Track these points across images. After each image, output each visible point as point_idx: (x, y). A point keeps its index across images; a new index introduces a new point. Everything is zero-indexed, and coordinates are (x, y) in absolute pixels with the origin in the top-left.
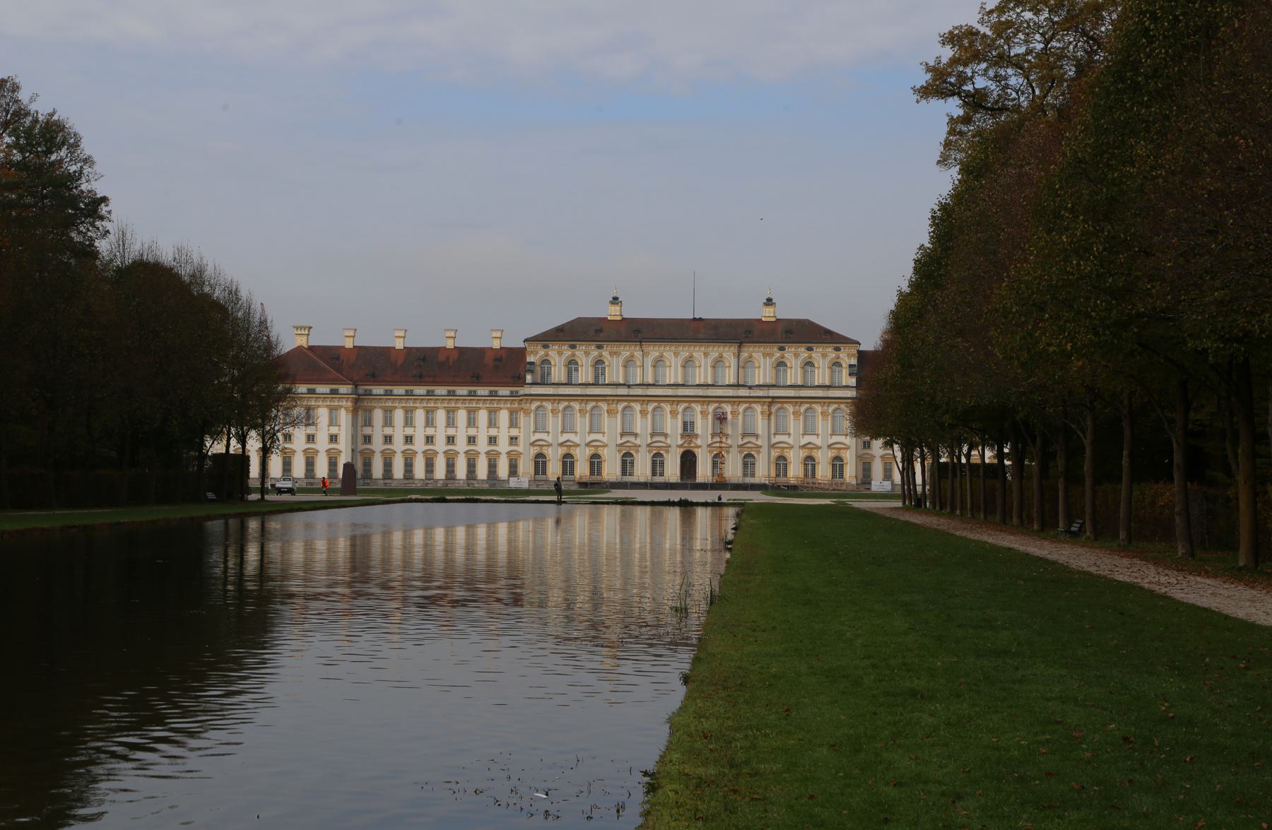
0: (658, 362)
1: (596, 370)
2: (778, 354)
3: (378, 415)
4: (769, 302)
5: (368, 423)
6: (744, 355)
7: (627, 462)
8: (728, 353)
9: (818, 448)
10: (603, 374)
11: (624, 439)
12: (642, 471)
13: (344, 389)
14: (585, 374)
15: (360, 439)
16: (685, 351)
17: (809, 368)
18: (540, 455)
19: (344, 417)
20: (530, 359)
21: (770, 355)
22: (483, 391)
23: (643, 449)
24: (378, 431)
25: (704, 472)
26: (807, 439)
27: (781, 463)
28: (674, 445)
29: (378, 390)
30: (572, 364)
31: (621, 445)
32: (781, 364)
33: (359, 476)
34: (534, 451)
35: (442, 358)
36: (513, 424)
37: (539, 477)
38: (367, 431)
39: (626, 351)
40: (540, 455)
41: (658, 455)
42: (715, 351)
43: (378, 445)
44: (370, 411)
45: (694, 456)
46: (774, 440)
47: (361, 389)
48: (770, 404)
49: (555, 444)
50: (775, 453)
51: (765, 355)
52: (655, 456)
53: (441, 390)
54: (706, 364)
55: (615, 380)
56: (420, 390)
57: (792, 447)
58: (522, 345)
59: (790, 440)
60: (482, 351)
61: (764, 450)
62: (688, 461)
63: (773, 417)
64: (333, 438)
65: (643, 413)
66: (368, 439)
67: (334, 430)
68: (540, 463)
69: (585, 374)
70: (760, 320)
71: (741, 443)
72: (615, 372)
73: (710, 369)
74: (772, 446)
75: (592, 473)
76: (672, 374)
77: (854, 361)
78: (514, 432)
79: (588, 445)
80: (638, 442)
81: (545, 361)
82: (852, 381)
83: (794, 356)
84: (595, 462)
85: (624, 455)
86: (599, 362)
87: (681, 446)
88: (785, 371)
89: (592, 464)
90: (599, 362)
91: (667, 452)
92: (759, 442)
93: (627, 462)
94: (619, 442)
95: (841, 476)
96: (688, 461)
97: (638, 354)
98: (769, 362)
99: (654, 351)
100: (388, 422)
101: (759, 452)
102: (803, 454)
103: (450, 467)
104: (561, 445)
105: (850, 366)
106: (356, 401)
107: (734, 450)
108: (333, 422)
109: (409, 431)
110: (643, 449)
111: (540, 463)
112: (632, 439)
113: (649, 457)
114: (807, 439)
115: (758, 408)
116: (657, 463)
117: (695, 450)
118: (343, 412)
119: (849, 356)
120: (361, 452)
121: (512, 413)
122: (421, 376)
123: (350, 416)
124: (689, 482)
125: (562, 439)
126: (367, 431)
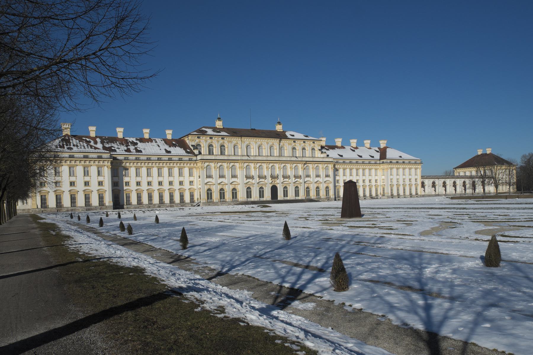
4: (279, 123)
11: (248, 180)
12: (255, 196)
18: (209, 190)
19: (107, 172)
31: (246, 183)
34: (206, 187)
36: (191, 175)
41: (261, 188)
51: (289, 144)
62: (274, 190)
64: (100, 183)
67: (101, 179)
77: (320, 148)
79: (231, 184)
80: (253, 181)
85: (247, 189)
88: (296, 152)
93: (249, 194)
94: (245, 182)
96: (274, 190)
97: (240, 142)
98: (290, 147)
104: (219, 184)
109: (139, 179)
117: (277, 185)
121: (190, 169)
125: (219, 182)
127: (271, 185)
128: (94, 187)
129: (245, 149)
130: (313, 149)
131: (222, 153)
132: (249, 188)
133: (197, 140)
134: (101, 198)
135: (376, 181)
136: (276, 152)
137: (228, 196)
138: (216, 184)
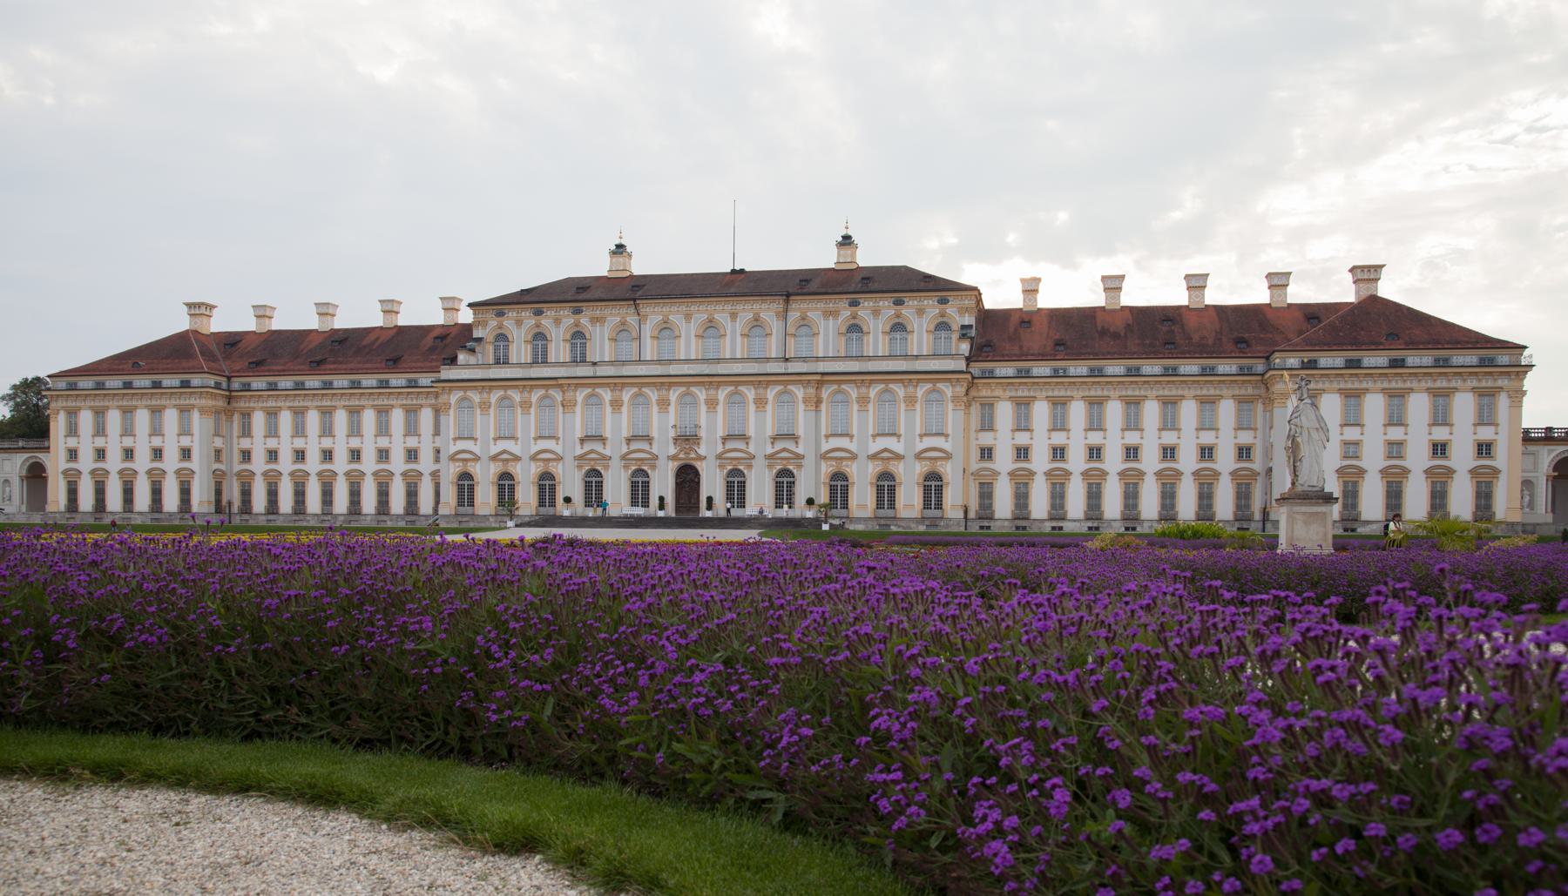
0: (665, 327)
1: (573, 346)
2: (846, 313)
3: (259, 420)
5: (246, 432)
6: (794, 316)
7: (594, 488)
8: (768, 311)
9: (899, 457)
13: (196, 380)
14: (559, 350)
15: (237, 456)
16: (701, 312)
17: (898, 335)
20: (477, 334)
21: (834, 314)
22: (397, 380)
23: (616, 463)
24: (258, 444)
26: (882, 443)
27: (839, 486)
28: (661, 462)
29: (258, 383)
31: (581, 457)
32: (855, 328)
33: (235, 509)
35: (372, 337)
37: (462, 510)
38: (245, 443)
39: (615, 315)
42: (747, 310)
43: (259, 464)
44: (247, 415)
45: (697, 474)
46: (825, 447)
47: (236, 384)
48: (820, 384)
49: (485, 458)
50: (826, 469)
51: (828, 314)
52: (588, 474)
53: (341, 381)
54: (733, 332)
56: (313, 382)
57: (854, 457)
59: (853, 447)
62: (687, 478)
63: (823, 407)
64: (186, 453)
65: (616, 405)
66: (246, 455)
67: (186, 441)
69: (559, 350)
71: (770, 450)
72: (601, 345)
73: (739, 339)
74: (824, 457)
75: (541, 503)
76: (688, 345)
77: (969, 320)
79: (534, 458)
80: (607, 452)
81: (502, 338)
82: (965, 347)
83: (876, 315)
84: (546, 487)
86: (578, 336)
87: (674, 458)
88: (860, 340)
89: (541, 488)
90: (578, 336)
91: (653, 467)
92: (800, 450)
93: (594, 488)
94: (579, 451)
95: (939, 506)
96: (687, 478)
97: (632, 320)
99: (654, 314)
100: (272, 432)
101: (800, 466)
102: (873, 469)
103: (355, 495)
105: (963, 327)
106: (229, 399)
107: (759, 463)
108: (185, 431)
110: (616, 463)
112: (598, 447)
114: (882, 443)
115: (799, 392)
116: (640, 491)
117: (698, 464)
118: (196, 415)
119: (963, 311)
120: (239, 474)
122: (319, 363)
123: (209, 422)
124: (691, 516)
125: (494, 450)
126: (245, 443)
127: (677, 464)
128: (171, 462)
130: (942, 326)
131: (579, 359)
132: (595, 473)
134: (185, 493)
135: (1244, 452)
137: (527, 498)
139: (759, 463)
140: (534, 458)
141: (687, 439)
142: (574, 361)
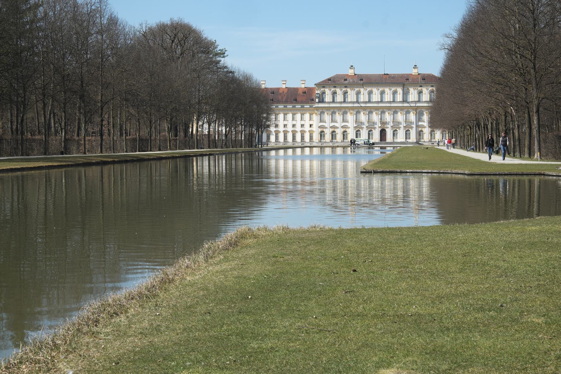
4: (415, 67)
6: (405, 89)
10: (347, 97)
14: (340, 98)
20: (317, 92)
22: (298, 106)
25: (389, 137)
30: (334, 93)
32: (420, 93)
34: (320, 130)
36: (311, 119)
40: (322, 132)
55: (353, 101)
58: (314, 86)
60: (296, 90)
61: (414, 129)
62: (383, 133)
68: (322, 134)
69: (340, 98)
70: (411, 74)
75: (344, 139)
78: (311, 123)
81: (324, 93)
96: (383, 133)
98: (416, 91)
111: (322, 134)
113: (367, 131)
117: (386, 130)
125: (332, 124)
127: (380, 129)
129: (367, 96)
133: (322, 89)
136: (399, 98)
138: (329, 127)
139: (402, 129)
140: (342, 127)
141: (383, 123)
142: (345, 102)
